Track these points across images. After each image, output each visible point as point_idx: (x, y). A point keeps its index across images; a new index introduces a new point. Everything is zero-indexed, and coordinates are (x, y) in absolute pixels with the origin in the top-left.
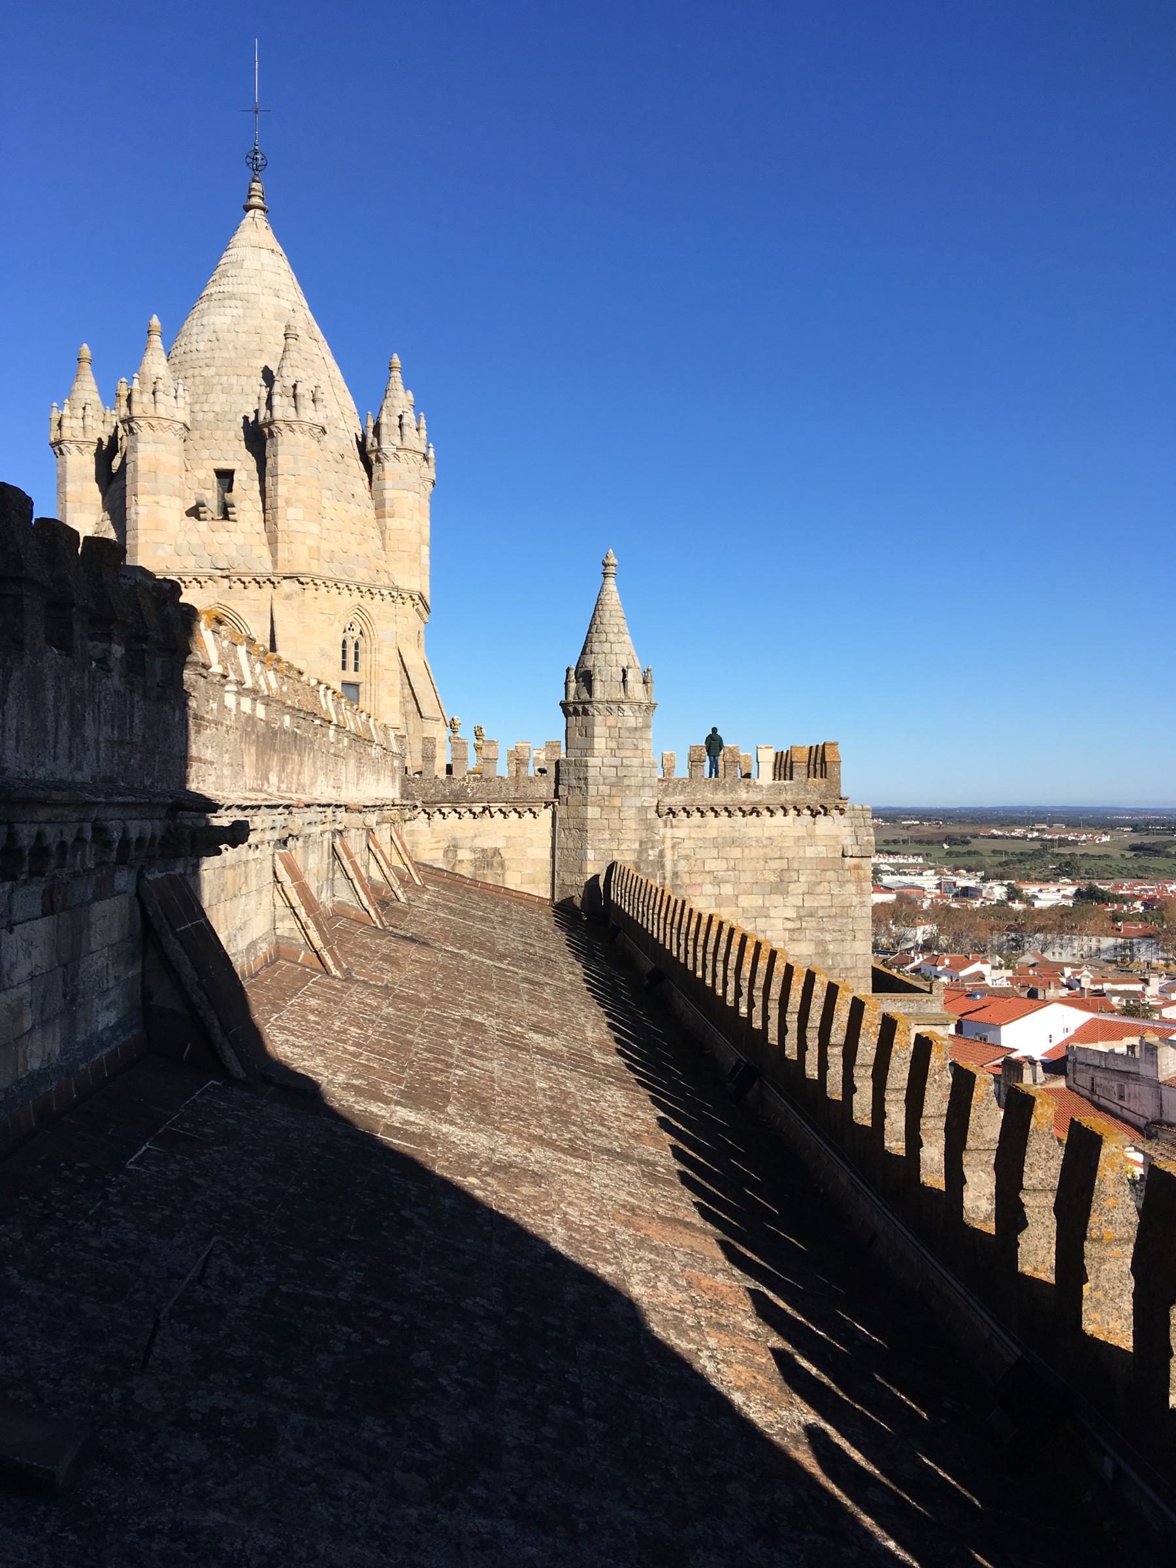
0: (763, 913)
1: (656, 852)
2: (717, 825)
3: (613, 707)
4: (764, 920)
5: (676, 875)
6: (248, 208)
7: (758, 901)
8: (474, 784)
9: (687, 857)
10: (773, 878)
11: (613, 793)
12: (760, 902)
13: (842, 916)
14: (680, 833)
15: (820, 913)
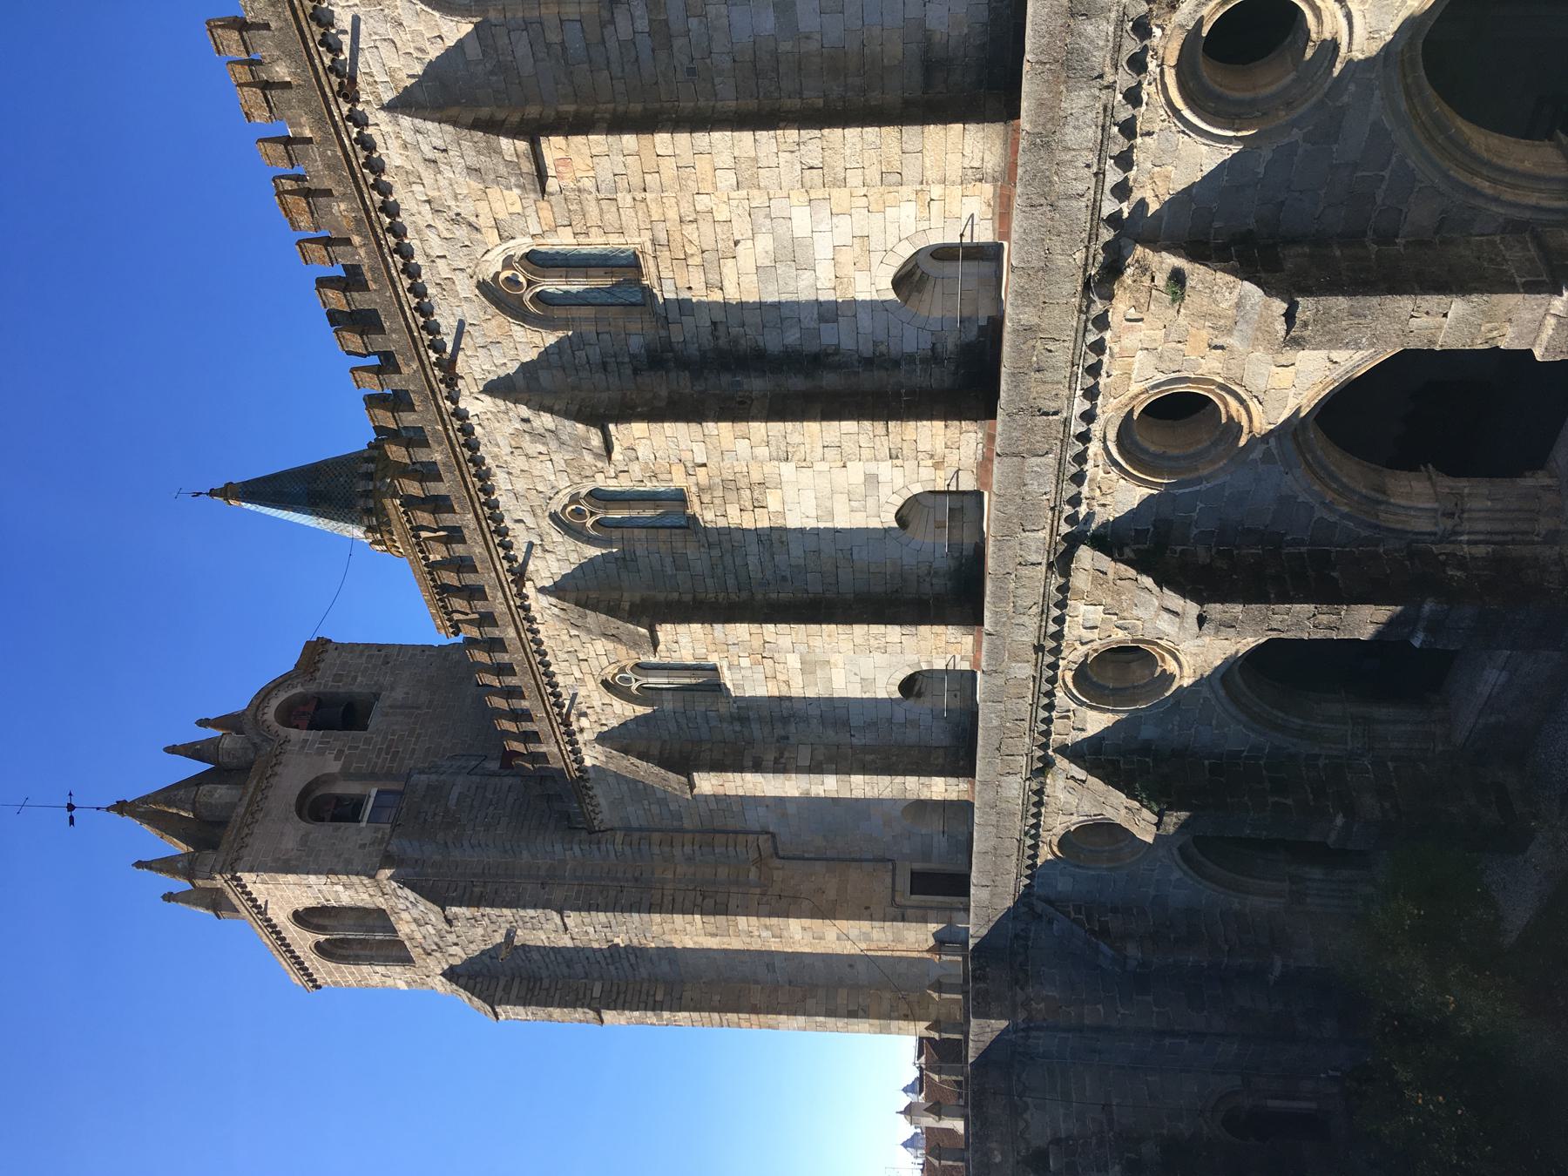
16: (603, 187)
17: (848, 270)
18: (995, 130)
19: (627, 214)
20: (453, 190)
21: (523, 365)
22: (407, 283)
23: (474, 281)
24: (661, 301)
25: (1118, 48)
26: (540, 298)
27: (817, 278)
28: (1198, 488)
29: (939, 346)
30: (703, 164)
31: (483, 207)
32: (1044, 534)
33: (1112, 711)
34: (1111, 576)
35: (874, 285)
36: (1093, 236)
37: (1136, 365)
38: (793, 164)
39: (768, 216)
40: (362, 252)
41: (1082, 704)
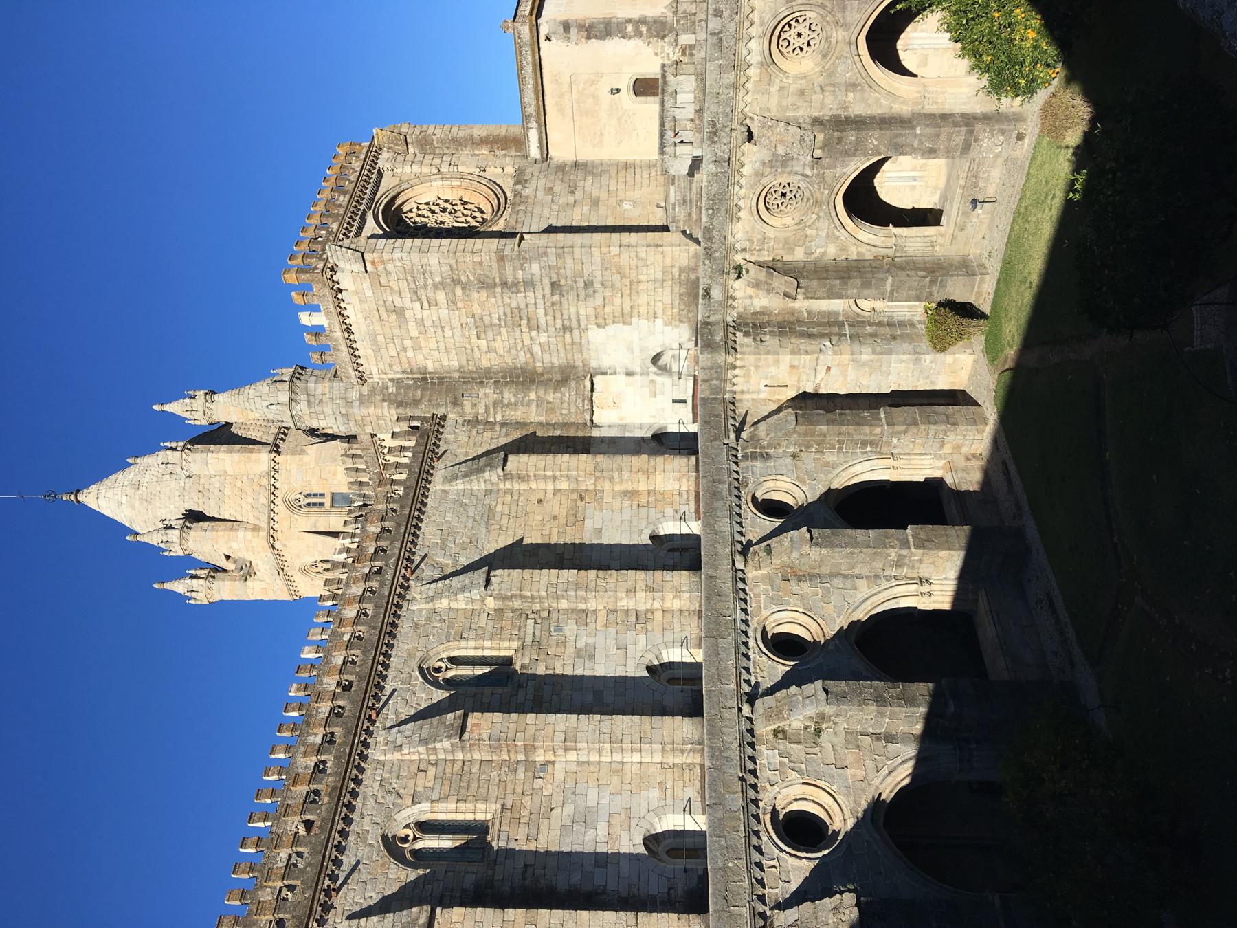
0: (420, 322)
1: (390, 384)
2: (363, 349)
3: (296, 418)
4: (425, 322)
5: (404, 372)
6: (79, 502)
7: (412, 326)
8: (371, 469)
9: (391, 366)
10: (393, 316)
11: (353, 419)
12: (414, 324)
13: (412, 273)
14: (375, 370)
15: (413, 286)
16: (493, 737)
17: (616, 830)
18: (699, 719)
19: (493, 788)
20: (399, 773)
21: (384, 898)
22: (341, 825)
23: (380, 832)
24: (495, 848)
25: (730, 491)
26: (415, 853)
27: (597, 835)
28: (808, 666)
29: (672, 891)
30: (549, 730)
31: (411, 783)
32: (733, 686)
33: (806, 858)
34: (774, 706)
35: (630, 843)
36: (732, 544)
37: (762, 602)
38: (595, 731)
39: (574, 793)
40: (323, 808)
41: (783, 851)
